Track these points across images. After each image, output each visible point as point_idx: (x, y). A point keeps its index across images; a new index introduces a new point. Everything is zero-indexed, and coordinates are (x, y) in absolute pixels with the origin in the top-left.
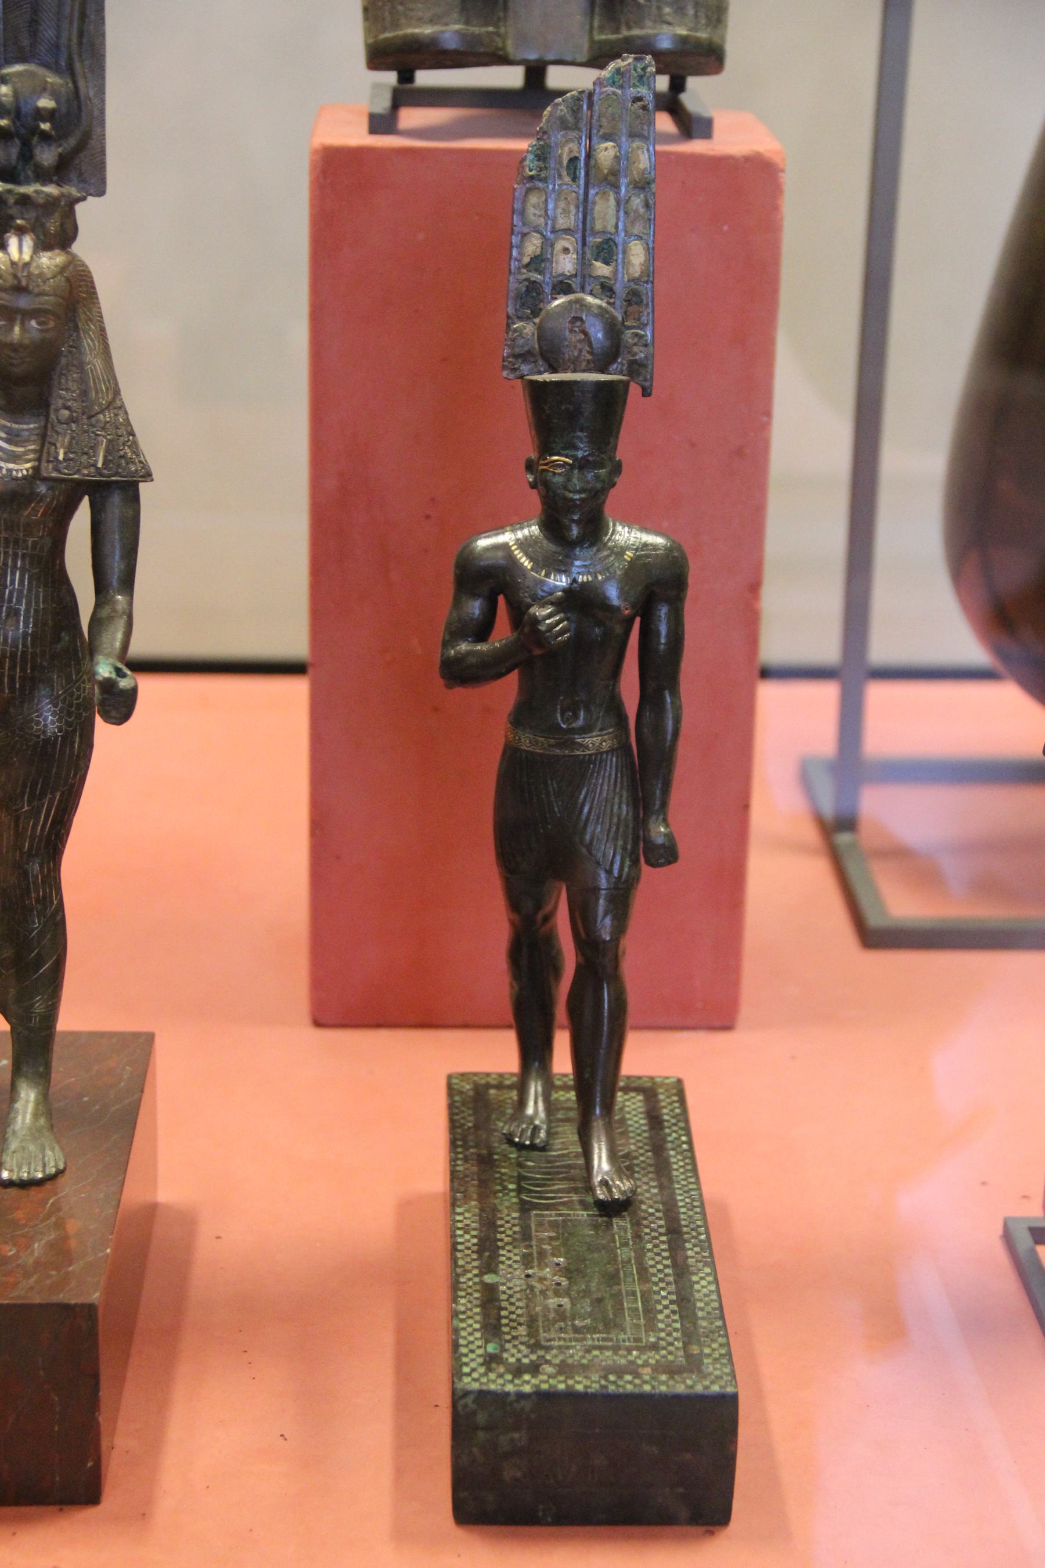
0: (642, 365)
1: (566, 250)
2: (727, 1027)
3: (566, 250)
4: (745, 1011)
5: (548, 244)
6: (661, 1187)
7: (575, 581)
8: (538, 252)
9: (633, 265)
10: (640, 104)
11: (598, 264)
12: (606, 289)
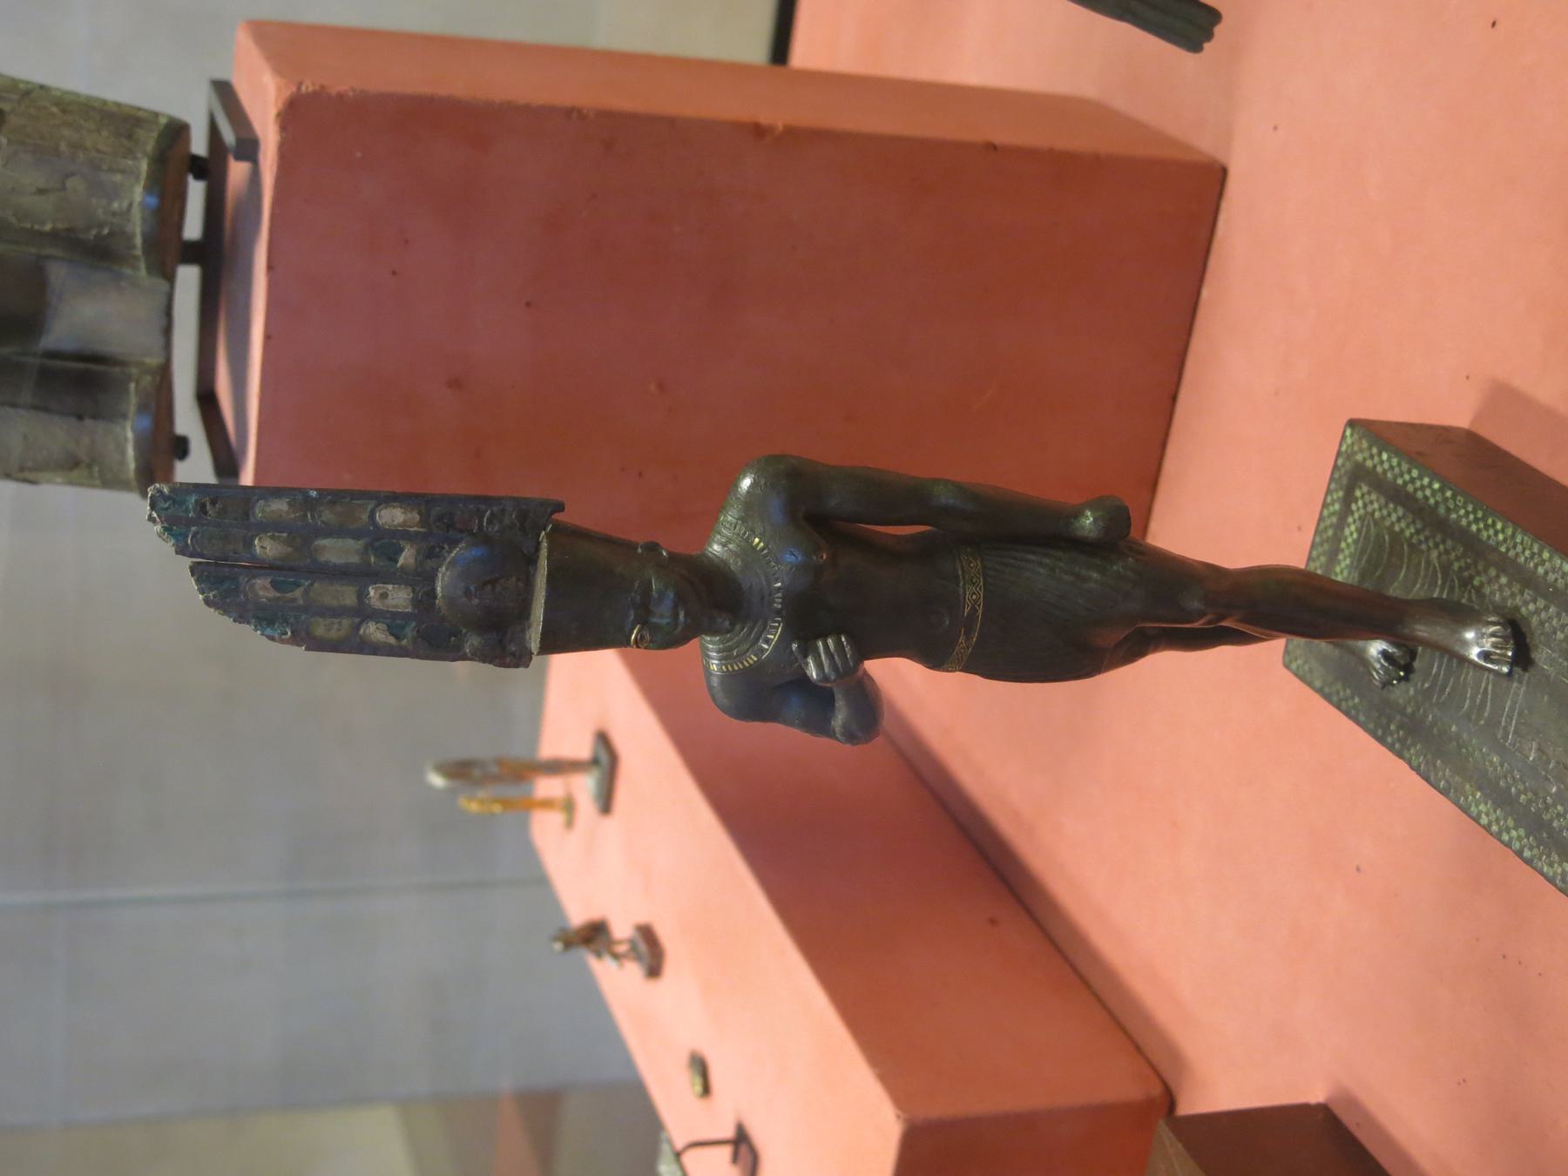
0: (523, 515)
1: (384, 596)
2: (1223, 172)
3: (384, 596)
4: (1205, 143)
5: (376, 615)
6: (1502, 570)
7: (778, 612)
8: (384, 627)
9: (404, 524)
10: (208, 507)
11: (401, 561)
12: (431, 554)
